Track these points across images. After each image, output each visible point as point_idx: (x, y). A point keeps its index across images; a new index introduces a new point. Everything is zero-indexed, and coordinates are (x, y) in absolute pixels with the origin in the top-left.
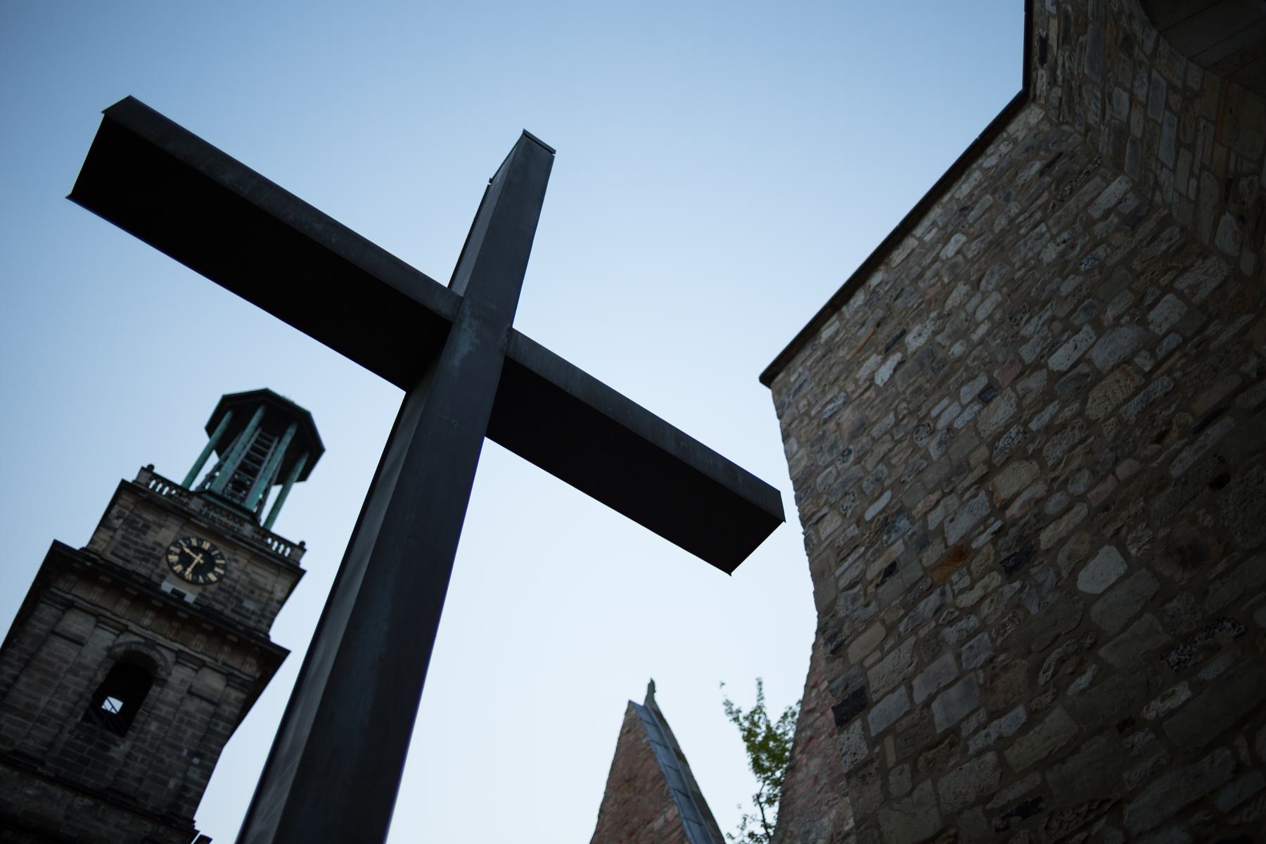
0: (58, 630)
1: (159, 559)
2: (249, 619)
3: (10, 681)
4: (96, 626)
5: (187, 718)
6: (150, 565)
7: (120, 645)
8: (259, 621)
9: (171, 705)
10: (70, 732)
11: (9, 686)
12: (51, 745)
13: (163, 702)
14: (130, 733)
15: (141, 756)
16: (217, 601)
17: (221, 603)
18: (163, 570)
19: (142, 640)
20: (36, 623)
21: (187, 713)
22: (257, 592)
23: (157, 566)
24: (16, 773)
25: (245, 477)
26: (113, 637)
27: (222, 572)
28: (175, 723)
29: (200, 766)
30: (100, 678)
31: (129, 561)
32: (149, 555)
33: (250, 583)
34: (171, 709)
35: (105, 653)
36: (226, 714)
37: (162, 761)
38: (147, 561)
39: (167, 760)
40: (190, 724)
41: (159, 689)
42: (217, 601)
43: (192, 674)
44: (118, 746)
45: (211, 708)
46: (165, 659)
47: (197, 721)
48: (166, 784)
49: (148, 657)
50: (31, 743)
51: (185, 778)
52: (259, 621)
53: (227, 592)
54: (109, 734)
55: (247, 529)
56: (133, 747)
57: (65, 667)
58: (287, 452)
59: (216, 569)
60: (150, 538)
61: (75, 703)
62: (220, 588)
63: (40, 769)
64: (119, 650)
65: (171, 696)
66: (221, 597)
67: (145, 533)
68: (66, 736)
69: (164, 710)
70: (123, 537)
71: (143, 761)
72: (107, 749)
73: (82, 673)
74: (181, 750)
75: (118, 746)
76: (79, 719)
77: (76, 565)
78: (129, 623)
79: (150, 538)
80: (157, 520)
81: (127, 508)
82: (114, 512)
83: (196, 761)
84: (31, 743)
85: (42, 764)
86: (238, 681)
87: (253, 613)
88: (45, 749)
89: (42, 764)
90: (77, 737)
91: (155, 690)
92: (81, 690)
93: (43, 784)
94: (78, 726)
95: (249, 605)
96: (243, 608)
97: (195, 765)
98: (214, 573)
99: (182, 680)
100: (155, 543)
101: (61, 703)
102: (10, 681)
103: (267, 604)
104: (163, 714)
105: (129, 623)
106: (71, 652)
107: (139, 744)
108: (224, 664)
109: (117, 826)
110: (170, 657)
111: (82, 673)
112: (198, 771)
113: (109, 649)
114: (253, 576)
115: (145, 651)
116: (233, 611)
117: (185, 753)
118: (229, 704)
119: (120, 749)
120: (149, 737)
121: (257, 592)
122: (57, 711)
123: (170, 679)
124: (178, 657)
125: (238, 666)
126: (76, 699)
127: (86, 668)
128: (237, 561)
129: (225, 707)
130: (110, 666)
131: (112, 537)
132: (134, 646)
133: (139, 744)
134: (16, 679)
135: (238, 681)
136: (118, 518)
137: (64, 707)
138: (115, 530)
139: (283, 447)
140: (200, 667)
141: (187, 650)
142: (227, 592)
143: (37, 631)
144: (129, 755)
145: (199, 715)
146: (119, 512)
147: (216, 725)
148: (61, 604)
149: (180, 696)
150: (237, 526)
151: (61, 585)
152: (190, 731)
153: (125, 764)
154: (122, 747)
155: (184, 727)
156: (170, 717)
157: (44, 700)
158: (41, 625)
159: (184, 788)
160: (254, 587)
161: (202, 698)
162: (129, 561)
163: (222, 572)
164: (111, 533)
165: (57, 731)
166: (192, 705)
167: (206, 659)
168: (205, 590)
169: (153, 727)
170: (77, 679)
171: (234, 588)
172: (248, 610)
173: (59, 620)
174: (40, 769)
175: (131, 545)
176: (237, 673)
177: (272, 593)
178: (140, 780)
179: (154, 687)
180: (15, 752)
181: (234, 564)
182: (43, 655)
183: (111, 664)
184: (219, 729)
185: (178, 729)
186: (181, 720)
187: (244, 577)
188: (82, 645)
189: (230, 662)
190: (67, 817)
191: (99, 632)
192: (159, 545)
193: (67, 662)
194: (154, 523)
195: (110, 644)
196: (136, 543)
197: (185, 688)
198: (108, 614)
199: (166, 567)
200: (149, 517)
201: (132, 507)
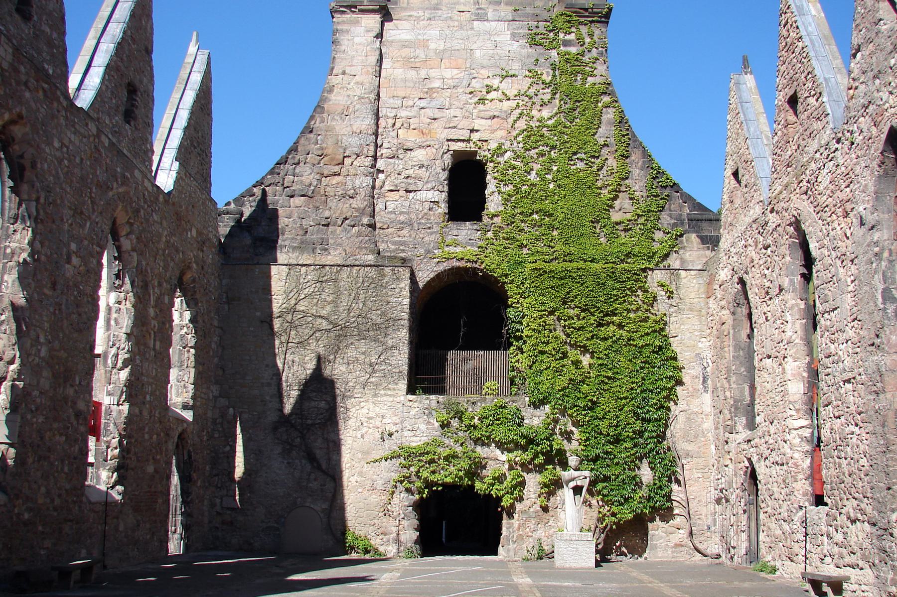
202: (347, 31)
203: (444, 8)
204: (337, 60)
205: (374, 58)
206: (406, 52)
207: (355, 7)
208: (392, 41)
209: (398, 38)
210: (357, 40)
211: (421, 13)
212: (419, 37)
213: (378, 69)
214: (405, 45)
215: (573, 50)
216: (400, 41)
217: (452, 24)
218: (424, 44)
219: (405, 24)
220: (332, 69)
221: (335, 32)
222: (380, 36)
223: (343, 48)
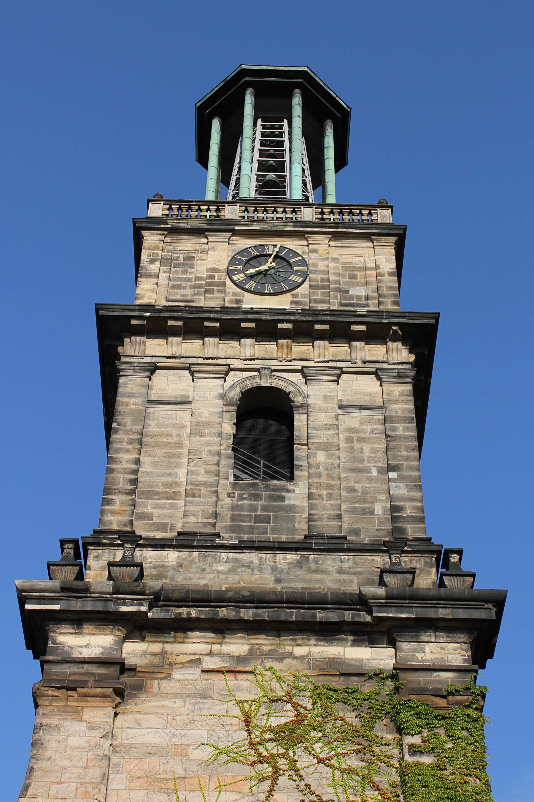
0: (153, 398)
1: (224, 284)
2: (367, 305)
3: (134, 467)
4: (194, 378)
5: (355, 436)
6: (216, 295)
7: (232, 387)
8: (380, 303)
9: (327, 427)
10: (229, 496)
11: (135, 472)
12: (216, 515)
13: (315, 428)
14: (296, 473)
15: (324, 492)
16: (317, 301)
17: (323, 302)
18: (234, 294)
19: (256, 373)
20: (126, 400)
21: (351, 430)
22: (359, 274)
23: (225, 292)
24: (195, 554)
25: (271, 175)
26: (221, 382)
27: (305, 269)
28: (342, 445)
29: (401, 478)
30: (229, 429)
31: (192, 301)
32: (210, 286)
33: (345, 268)
34: (330, 432)
35: (220, 402)
36: (400, 414)
37: (352, 490)
38: (211, 292)
39: (357, 487)
40: (361, 440)
41: (304, 417)
42: (317, 301)
43: (334, 385)
44: (293, 491)
45: (378, 415)
46: (293, 383)
47: (368, 435)
48: (372, 512)
49: (272, 389)
50: (192, 519)
51: (391, 498)
52: (380, 303)
53: (323, 287)
54: (275, 482)
55: (308, 214)
56: (310, 485)
57: (186, 432)
58: (305, 134)
59: (296, 269)
60: (201, 268)
61: (218, 464)
62: (311, 287)
63: (218, 541)
64: (235, 394)
65: (322, 418)
66: (319, 294)
67: (192, 266)
68: (227, 502)
69: (323, 436)
70: (169, 279)
71: (330, 496)
72: (282, 498)
73: (206, 431)
74: (368, 471)
75: (293, 491)
76: (232, 479)
77: (134, 322)
78: (229, 361)
79: (201, 268)
80: (197, 247)
81: (156, 248)
82: (144, 257)
83: (392, 475)
84: (192, 519)
85: (218, 536)
86: (394, 373)
87: (367, 298)
88: (212, 521)
89: (218, 536)
90: (241, 498)
91: (300, 421)
92: (216, 448)
93: (230, 555)
94: (234, 485)
95: (354, 291)
96: (352, 297)
97: (394, 480)
98: (296, 273)
99: (325, 397)
100: (209, 270)
101: (202, 469)
102: (134, 467)
103: (378, 282)
104: (324, 440)
105: (229, 361)
106: (183, 415)
107: (315, 480)
108: (365, 362)
109: (340, 571)
110: (297, 378)
111: (206, 431)
112: (401, 485)
113: (222, 396)
114: (343, 259)
115: (265, 383)
116: (341, 305)
117: (374, 472)
118: (396, 402)
119: (297, 493)
120: (321, 469)
121: (359, 274)
122: (202, 478)
123: (310, 401)
124: (305, 376)
125: (381, 359)
126: (216, 459)
127: (208, 424)
128: (315, 251)
129: (393, 407)
130: (234, 414)
131: (157, 284)
132: (249, 385)
133: (315, 480)
134: (137, 462)
135: (390, 373)
136: (152, 262)
137: (207, 472)
138: (157, 275)
139: (297, 122)
140: (339, 377)
141: (312, 364)
142: (323, 287)
143: (134, 407)
144: (310, 496)
145: (368, 428)
146: (149, 256)
147: (394, 429)
148: (141, 370)
149: (333, 415)
150: (293, 216)
151: (130, 352)
152: (367, 448)
153: (311, 507)
154: (297, 491)
155: (356, 445)
156: (335, 440)
157: (182, 476)
158: (133, 400)
159: (395, 509)
160: (352, 272)
161: (361, 408)
162: (192, 301)
163: (305, 269)
164: (155, 280)
165: (214, 499)
166: (353, 420)
167: (339, 364)
168: (295, 296)
169: (321, 457)
170: (204, 439)
171: (328, 280)
172: (359, 298)
173: (149, 388)
174: (218, 541)
175: (183, 284)
176: (385, 366)
177: (377, 268)
178: (339, 517)
179: (296, 417)
180: (180, 534)
181: (314, 256)
182: (152, 427)
183: (233, 411)
184: (400, 432)
185: (351, 450)
186: (350, 440)
187: (332, 265)
188: (190, 403)
189: (368, 358)
190: (278, 581)
191: (200, 382)
192: (215, 270)
193: (184, 427)
194: (196, 251)
195: (221, 391)
196: (189, 280)
197: (335, 405)
198: (200, 361)
199: (238, 290)
200: (186, 245)
201: (161, 245)
202: (58, 728)
203: (215, 695)
204: (36, 774)
205: (95, 773)
206: (153, 763)
207: (74, 689)
208: (130, 747)
209: (139, 741)
210: (73, 741)
211: (179, 703)
212: (176, 741)
213: (103, 788)
214: (150, 752)
215: (427, 760)
216: (143, 746)
217: (228, 721)
218: (181, 752)
219: (153, 720)
220: (26, 787)
221: (37, 728)
222: (110, 735)
223: (48, 754)
